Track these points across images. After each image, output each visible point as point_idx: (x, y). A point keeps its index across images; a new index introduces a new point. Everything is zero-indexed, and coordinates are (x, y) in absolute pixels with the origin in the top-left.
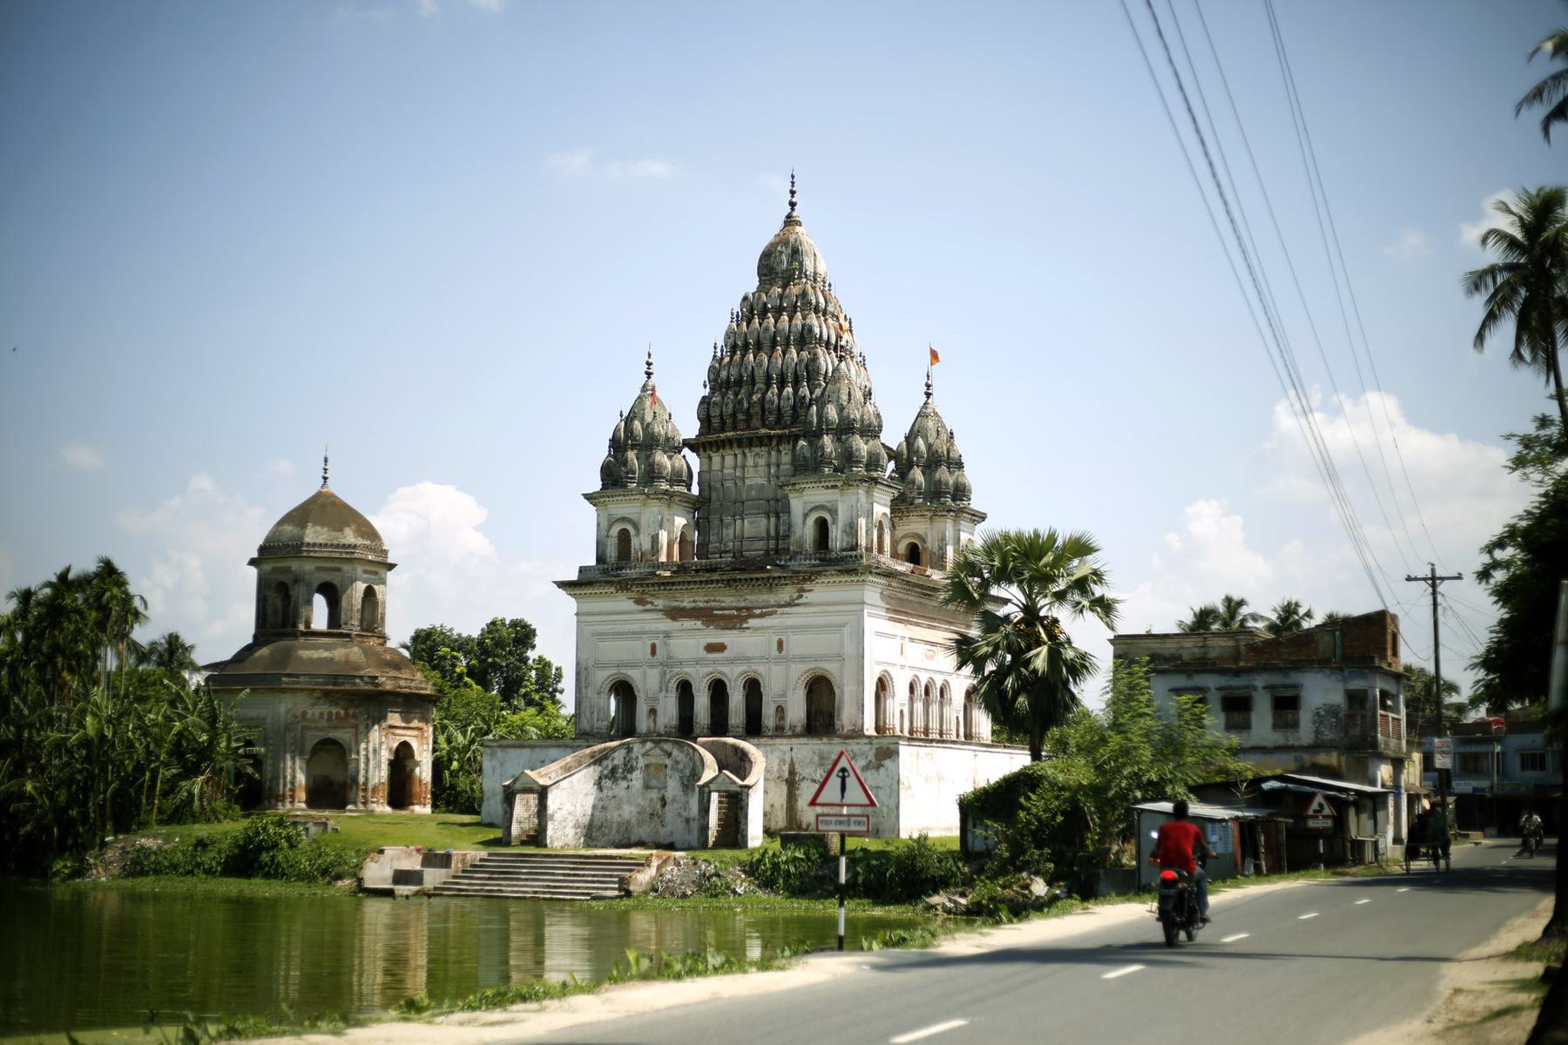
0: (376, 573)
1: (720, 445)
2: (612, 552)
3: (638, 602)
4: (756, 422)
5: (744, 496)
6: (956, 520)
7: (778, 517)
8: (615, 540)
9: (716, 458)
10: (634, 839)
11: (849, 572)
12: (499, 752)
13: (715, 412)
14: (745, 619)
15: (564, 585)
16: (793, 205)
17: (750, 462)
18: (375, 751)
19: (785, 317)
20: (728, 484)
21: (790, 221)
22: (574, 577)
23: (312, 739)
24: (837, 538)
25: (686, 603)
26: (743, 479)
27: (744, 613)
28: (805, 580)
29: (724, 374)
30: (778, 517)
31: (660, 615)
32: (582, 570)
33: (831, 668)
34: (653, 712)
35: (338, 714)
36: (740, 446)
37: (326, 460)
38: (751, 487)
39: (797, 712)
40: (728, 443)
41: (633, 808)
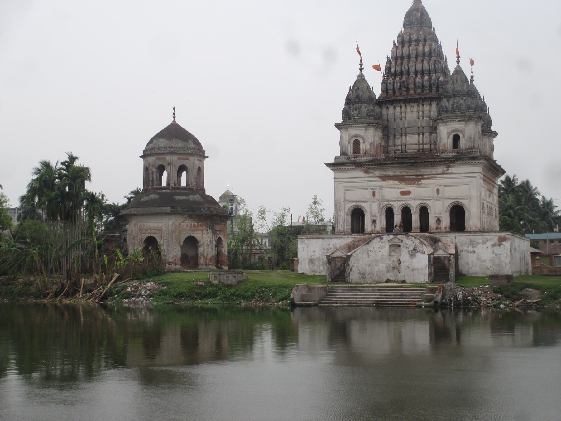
0: (201, 161)
1: (393, 102)
3: (365, 172)
4: (412, 92)
5: (406, 126)
6: (489, 136)
7: (423, 134)
9: (391, 109)
10: (385, 279)
11: (474, 158)
12: (306, 241)
15: (329, 165)
17: (409, 109)
18: (211, 241)
19: (421, 44)
20: (398, 120)
22: (333, 161)
23: (184, 237)
24: (463, 143)
25: (391, 173)
26: (406, 118)
27: (420, 177)
28: (451, 162)
29: (393, 70)
30: (423, 134)
31: (377, 179)
32: (336, 158)
33: (465, 203)
34: (374, 222)
35: (194, 225)
37: (174, 109)
38: (409, 121)
39: (446, 221)
40: (400, 101)
41: (384, 265)
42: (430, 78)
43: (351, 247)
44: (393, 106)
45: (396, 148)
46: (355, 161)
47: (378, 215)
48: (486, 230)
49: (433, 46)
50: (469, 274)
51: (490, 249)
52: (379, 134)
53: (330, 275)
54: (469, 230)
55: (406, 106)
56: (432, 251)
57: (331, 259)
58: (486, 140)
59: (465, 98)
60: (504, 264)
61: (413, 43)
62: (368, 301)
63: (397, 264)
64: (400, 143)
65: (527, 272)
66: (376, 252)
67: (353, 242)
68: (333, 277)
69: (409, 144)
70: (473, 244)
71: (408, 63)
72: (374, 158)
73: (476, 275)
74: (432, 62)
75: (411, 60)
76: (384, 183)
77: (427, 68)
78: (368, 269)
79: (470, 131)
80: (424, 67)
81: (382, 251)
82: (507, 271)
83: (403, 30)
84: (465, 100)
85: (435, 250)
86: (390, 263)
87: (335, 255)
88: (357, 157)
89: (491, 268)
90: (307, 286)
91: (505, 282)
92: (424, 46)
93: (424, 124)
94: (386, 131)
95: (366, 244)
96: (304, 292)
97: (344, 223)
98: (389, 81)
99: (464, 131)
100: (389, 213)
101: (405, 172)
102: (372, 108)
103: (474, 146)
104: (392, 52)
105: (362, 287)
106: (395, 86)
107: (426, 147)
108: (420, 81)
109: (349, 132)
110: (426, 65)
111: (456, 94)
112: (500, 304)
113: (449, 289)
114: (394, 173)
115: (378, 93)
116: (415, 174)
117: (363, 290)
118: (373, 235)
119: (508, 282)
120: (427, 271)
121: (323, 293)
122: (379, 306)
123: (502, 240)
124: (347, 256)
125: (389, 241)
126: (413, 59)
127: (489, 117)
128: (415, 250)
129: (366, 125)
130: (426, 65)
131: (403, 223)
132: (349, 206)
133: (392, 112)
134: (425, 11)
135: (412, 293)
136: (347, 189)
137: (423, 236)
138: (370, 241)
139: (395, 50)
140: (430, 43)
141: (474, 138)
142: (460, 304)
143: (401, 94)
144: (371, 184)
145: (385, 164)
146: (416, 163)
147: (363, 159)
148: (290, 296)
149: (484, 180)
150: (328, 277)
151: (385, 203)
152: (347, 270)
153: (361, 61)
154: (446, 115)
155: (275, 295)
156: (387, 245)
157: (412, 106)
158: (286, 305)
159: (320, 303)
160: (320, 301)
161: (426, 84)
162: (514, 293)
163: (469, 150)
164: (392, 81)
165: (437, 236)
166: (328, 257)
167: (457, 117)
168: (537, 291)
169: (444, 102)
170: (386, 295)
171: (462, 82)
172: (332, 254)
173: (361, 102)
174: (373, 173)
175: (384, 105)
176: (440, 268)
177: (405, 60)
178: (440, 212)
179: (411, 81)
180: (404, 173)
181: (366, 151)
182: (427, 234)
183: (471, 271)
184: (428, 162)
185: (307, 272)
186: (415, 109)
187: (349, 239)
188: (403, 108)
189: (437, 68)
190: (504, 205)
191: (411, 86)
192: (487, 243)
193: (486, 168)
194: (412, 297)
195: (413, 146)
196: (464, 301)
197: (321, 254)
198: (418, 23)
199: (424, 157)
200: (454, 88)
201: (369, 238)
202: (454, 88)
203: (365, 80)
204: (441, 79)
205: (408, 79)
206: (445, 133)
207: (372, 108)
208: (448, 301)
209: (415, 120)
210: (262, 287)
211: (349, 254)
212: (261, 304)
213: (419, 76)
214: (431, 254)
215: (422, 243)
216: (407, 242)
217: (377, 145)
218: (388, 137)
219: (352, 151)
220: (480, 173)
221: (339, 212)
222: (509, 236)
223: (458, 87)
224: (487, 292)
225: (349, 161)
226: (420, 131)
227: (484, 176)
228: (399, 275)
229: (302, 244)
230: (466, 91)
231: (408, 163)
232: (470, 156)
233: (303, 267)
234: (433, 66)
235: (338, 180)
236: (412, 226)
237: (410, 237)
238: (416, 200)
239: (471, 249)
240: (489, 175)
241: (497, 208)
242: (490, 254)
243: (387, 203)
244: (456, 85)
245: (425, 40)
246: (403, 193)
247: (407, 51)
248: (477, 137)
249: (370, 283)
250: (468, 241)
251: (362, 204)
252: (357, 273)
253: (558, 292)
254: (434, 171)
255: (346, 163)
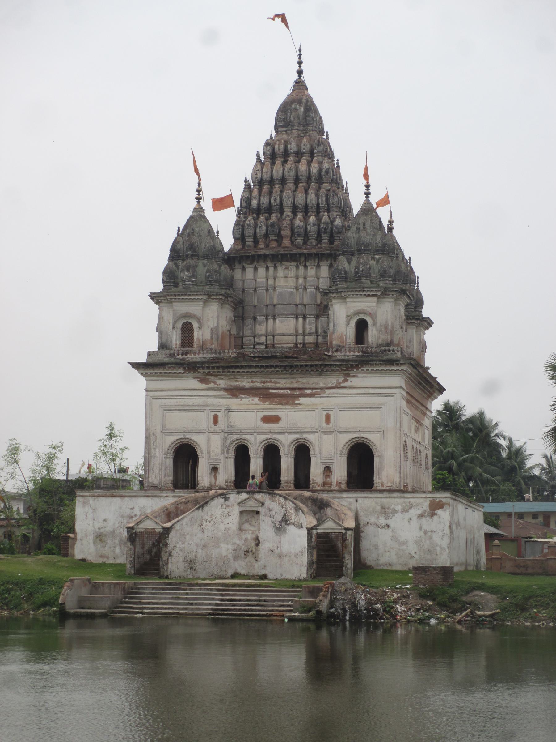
1: (254, 259)
2: (175, 339)
3: (201, 381)
4: (286, 242)
5: (275, 302)
7: (305, 318)
8: (179, 331)
9: (250, 271)
10: (230, 572)
11: (392, 362)
12: (91, 501)
13: (249, 232)
14: (298, 397)
15: (136, 365)
16: (300, 72)
17: (281, 272)
19: (304, 161)
21: (300, 85)
22: (143, 359)
24: (373, 336)
25: (246, 383)
26: (275, 288)
27: (297, 392)
28: (352, 367)
29: (255, 202)
30: (305, 318)
31: (222, 393)
32: (150, 354)
33: (374, 439)
34: (215, 469)
36: (272, 262)
38: (281, 294)
39: (340, 472)
40: (265, 257)
42: (319, 220)
43: (170, 514)
44: (253, 266)
45: (257, 340)
46: (184, 359)
47: (222, 457)
48: (410, 489)
49: (326, 165)
50: (378, 565)
51: (415, 523)
52: (228, 313)
53: (133, 562)
54: (380, 488)
55: (275, 267)
56: (315, 522)
57: (136, 534)
58: (412, 332)
59: (377, 257)
60: (438, 549)
61: (291, 158)
62: (199, 609)
63: (253, 545)
64: (264, 332)
65: (477, 566)
66: (215, 523)
67: (176, 504)
68: (137, 566)
69: (279, 334)
70: (385, 511)
71: (282, 191)
72: (218, 355)
73: (389, 568)
74: (322, 192)
75: (286, 187)
76: (234, 402)
77: (315, 202)
78: (201, 554)
79: (385, 313)
80: (309, 199)
81: (226, 521)
82: (443, 559)
83: (274, 134)
84: (378, 261)
85: (320, 522)
86: (241, 543)
87: (142, 526)
88: (187, 353)
89: (417, 556)
90: (89, 580)
91: (439, 579)
92: (309, 163)
93: (306, 300)
94: (240, 309)
95: (198, 508)
96: (84, 592)
97: (161, 469)
98: (247, 222)
99: (375, 314)
100: (242, 454)
101: (271, 382)
102: (215, 267)
103: (392, 342)
104: (255, 172)
105: (189, 585)
106: (258, 231)
107: (310, 339)
108: (302, 224)
109: (175, 308)
110: (312, 196)
111: (363, 249)
112: (429, 618)
113: (343, 589)
114: (252, 384)
115: (227, 242)
116: (288, 386)
117: (190, 590)
118: (212, 492)
119: (444, 580)
120: (304, 559)
121: (119, 595)
122: (220, 619)
123: (436, 506)
124: (164, 528)
125: (239, 504)
126: (290, 185)
127: (418, 292)
128: (285, 520)
129: (205, 297)
130: (312, 196)
131: (266, 471)
132: (170, 440)
133: (252, 276)
134: (313, 104)
135: (277, 596)
136: (168, 410)
137: (301, 496)
138: (206, 503)
139: (259, 168)
140: (320, 159)
141: (392, 326)
142: (360, 616)
143: (267, 246)
144: (210, 401)
145: (236, 367)
146: (292, 366)
147: (198, 357)
148: (57, 599)
149: (408, 402)
150: (128, 566)
151: (235, 437)
152: (163, 553)
153: (199, 184)
154: (344, 285)
155: (30, 596)
156: (236, 510)
157: (287, 268)
158: (50, 615)
159: (113, 612)
160: (113, 609)
161: (312, 229)
162: (454, 600)
163: (383, 348)
164: (252, 222)
165: (325, 496)
166: (130, 529)
167: (363, 289)
168: (494, 597)
169: (343, 263)
170: (231, 600)
171: (374, 228)
172: (137, 524)
173: (198, 255)
174: (215, 383)
175: (237, 265)
176: (327, 553)
177: (277, 187)
178: (330, 456)
179: (286, 223)
180: (269, 385)
181: (204, 343)
182: (306, 494)
183: (382, 560)
184: (311, 366)
185: (92, 558)
186: (292, 273)
187: (168, 500)
188: (271, 270)
189: (331, 202)
190: (442, 451)
191: (286, 232)
192: (411, 511)
193: (409, 379)
194: (276, 603)
195: (286, 338)
196: (369, 611)
197: (117, 525)
198: (299, 124)
199: (305, 357)
200: (359, 239)
201: (205, 497)
202: (359, 238)
203: (205, 218)
204: (338, 222)
205: (280, 219)
206: (342, 316)
207: (215, 267)
208: (340, 611)
209: (292, 292)
210: (8, 582)
211: (168, 525)
212: (5, 613)
213: (300, 215)
214: (312, 529)
215: (297, 509)
216: (271, 507)
217: (223, 333)
218: (243, 320)
219: (179, 342)
220: (401, 387)
221: (152, 451)
222: (449, 500)
223: (366, 237)
224: (408, 596)
225: (172, 360)
226: (299, 312)
227: (407, 393)
228: (256, 565)
229: (84, 507)
230: (380, 245)
231: (277, 366)
232: (385, 358)
233: (84, 548)
234: (324, 199)
235: (152, 394)
236: (282, 478)
237: (277, 498)
238: (290, 433)
239: (382, 521)
240: (418, 393)
241: (429, 453)
242: (415, 530)
243: (238, 436)
244: (363, 234)
245: (312, 154)
246: (267, 419)
247: (281, 172)
248: (397, 326)
249: (204, 579)
250: (378, 508)
251: (194, 438)
252: (182, 559)
253: (530, 597)
254: (321, 382)
255: (168, 364)
